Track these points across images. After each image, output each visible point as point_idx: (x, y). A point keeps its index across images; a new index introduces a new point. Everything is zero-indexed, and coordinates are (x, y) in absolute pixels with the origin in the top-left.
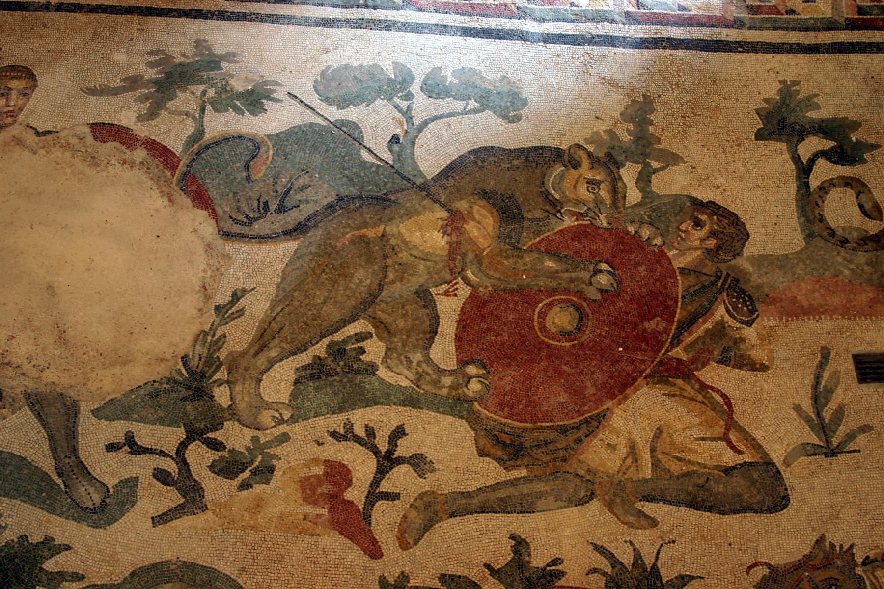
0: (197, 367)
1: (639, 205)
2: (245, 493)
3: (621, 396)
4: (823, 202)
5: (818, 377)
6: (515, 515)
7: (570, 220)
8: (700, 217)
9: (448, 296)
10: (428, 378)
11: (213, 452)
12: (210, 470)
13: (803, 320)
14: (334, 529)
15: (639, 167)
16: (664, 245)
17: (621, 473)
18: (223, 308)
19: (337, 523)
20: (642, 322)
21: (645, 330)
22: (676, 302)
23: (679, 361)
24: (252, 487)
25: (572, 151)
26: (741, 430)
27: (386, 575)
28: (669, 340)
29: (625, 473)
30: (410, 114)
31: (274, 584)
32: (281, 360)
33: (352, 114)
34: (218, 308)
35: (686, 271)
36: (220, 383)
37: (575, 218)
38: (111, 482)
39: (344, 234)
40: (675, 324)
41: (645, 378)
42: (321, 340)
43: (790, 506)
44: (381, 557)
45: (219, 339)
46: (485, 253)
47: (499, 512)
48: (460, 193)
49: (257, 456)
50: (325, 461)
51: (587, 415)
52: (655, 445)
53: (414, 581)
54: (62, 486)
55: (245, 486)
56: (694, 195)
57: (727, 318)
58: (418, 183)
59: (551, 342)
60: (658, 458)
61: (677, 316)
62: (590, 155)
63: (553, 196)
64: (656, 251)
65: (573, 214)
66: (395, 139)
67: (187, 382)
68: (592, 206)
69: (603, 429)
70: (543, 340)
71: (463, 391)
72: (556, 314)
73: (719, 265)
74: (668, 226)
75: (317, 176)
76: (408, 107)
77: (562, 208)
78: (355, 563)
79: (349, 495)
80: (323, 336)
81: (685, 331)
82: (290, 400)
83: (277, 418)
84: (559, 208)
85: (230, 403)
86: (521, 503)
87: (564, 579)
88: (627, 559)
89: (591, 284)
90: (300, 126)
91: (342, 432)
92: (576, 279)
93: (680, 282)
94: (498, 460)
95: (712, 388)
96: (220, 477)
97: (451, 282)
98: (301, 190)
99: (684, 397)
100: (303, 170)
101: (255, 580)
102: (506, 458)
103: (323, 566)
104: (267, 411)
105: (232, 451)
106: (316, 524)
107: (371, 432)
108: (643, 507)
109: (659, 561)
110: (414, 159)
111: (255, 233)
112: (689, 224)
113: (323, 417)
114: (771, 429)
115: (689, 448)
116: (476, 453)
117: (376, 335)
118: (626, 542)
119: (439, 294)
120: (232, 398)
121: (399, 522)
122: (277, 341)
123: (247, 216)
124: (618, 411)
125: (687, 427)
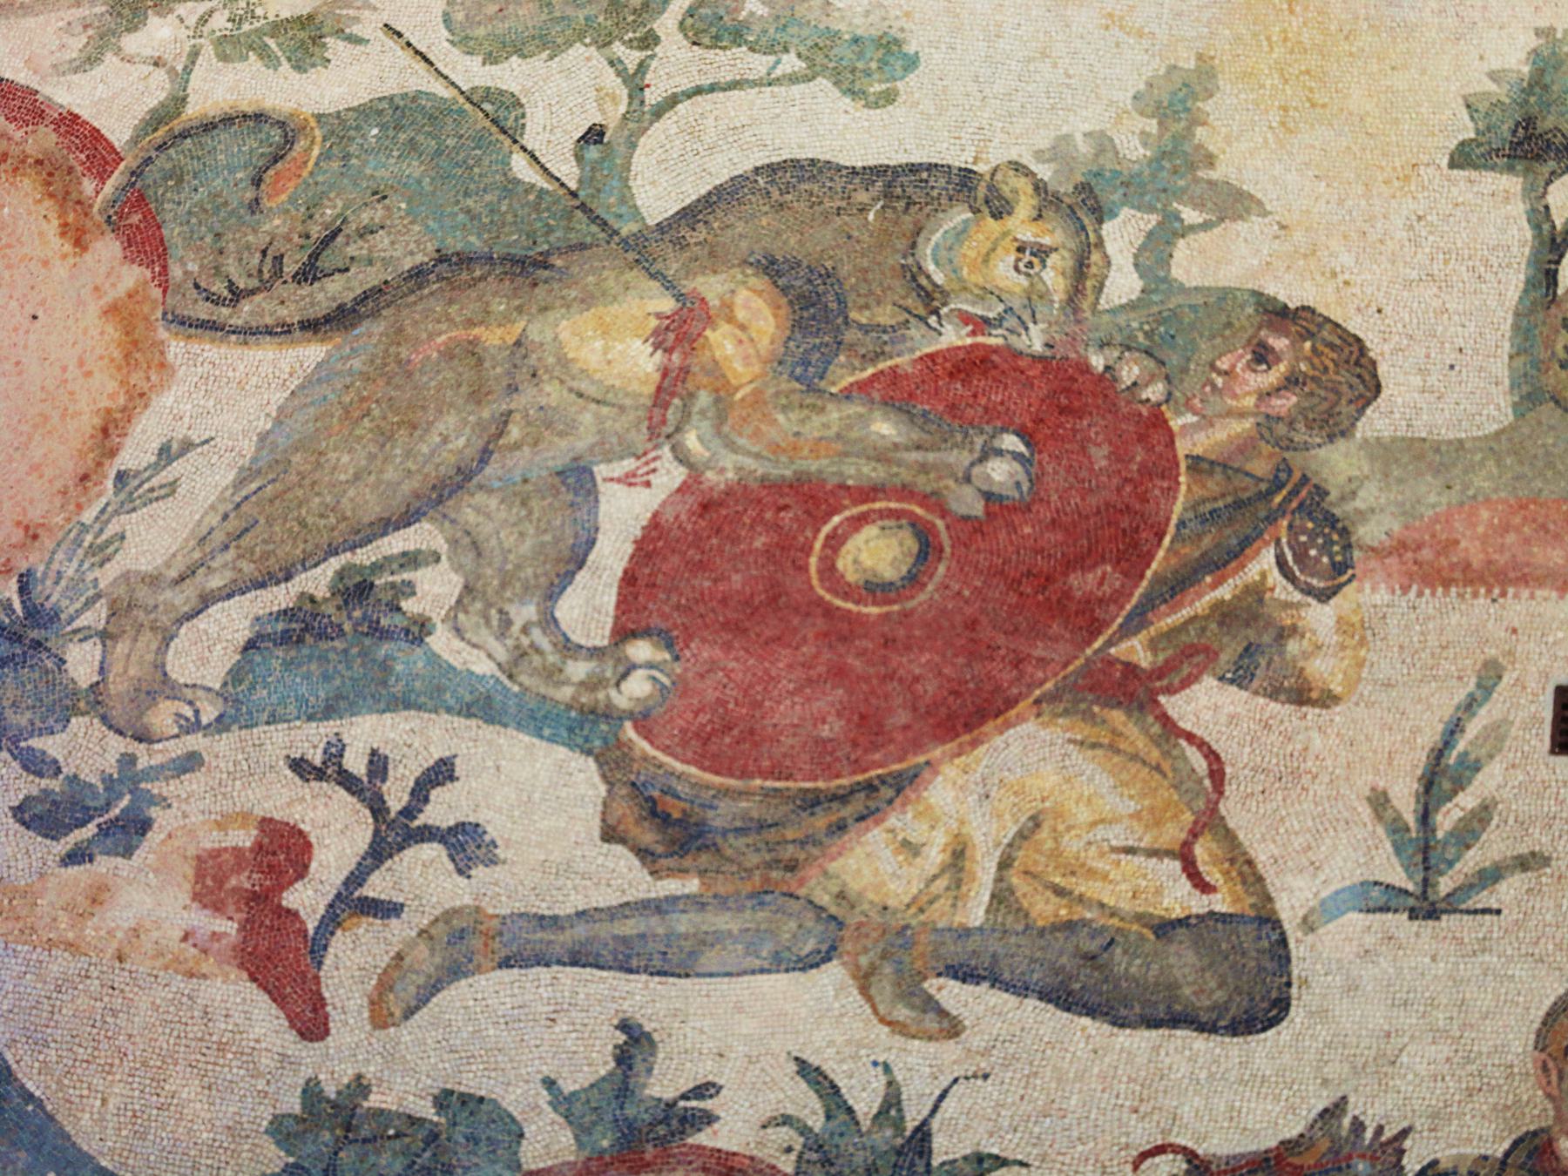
0: (48, 598)
1: (1131, 306)
2: (74, 870)
3: (966, 738)
5: (1454, 729)
6: (644, 977)
7: (957, 333)
8: (1271, 341)
9: (630, 484)
10: (537, 660)
11: (31, 777)
12: (15, 816)
13: (1461, 596)
14: (241, 966)
15: (1154, 219)
16: (1167, 401)
17: (913, 910)
18: (135, 477)
19: (250, 954)
20: (1066, 574)
21: (1067, 594)
22: (1160, 536)
23: (1131, 669)
24: (91, 861)
25: (999, 177)
26: (1230, 837)
27: (322, 1077)
28: (1120, 620)
29: (922, 910)
30: (642, 79)
31: (79, 1071)
32: (229, 596)
33: (510, 76)
34: (121, 477)
35: (1205, 466)
36: (84, 635)
37: (970, 328)
39: (431, 337)
41: (1037, 702)
42: (325, 560)
43: (1284, 1024)
44: (322, 1039)
45: (109, 542)
46: (739, 396)
47: (610, 968)
48: (715, 258)
49: (120, 796)
50: (264, 820)
51: (873, 773)
52: (1014, 854)
53: (379, 1097)
55: (76, 857)
56: (1271, 289)
57: (1275, 576)
58: (624, 232)
59: (839, 602)
61: (1154, 565)
62: (1039, 187)
63: (928, 277)
64: (1145, 412)
66: (595, 135)
67: (16, 628)
69: (904, 805)
70: (821, 598)
71: (608, 697)
72: (867, 542)
73: (1287, 455)
74: (1188, 360)
75: (403, 206)
76: (641, 65)
77: (944, 304)
78: (264, 1045)
80: (333, 551)
81: (1165, 601)
82: (225, 684)
83: (187, 719)
84: (936, 303)
85: (96, 678)
86: (665, 953)
87: (709, 1130)
88: (865, 1100)
89: (968, 479)
90: (391, 99)
91: (318, 762)
92: (935, 467)
94: (643, 853)
95: (1190, 737)
96: (31, 833)
97: (645, 454)
98: (361, 236)
99: (1118, 751)
100: (375, 193)
101: (41, 1058)
102: (660, 849)
103: (193, 1044)
104: (168, 703)
105: (74, 779)
106: (205, 952)
107: (378, 764)
108: (940, 989)
109: (938, 1116)
110: (627, 179)
111: (240, 322)
112: (1241, 356)
114: (1298, 842)
115: (1089, 870)
116: (597, 833)
117: (449, 558)
118: (875, 1064)
119: (612, 480)
120: (102, 668)
121: (383, 965)
122: (230, 555)
124: (950, 771)
125: (1102, 821)
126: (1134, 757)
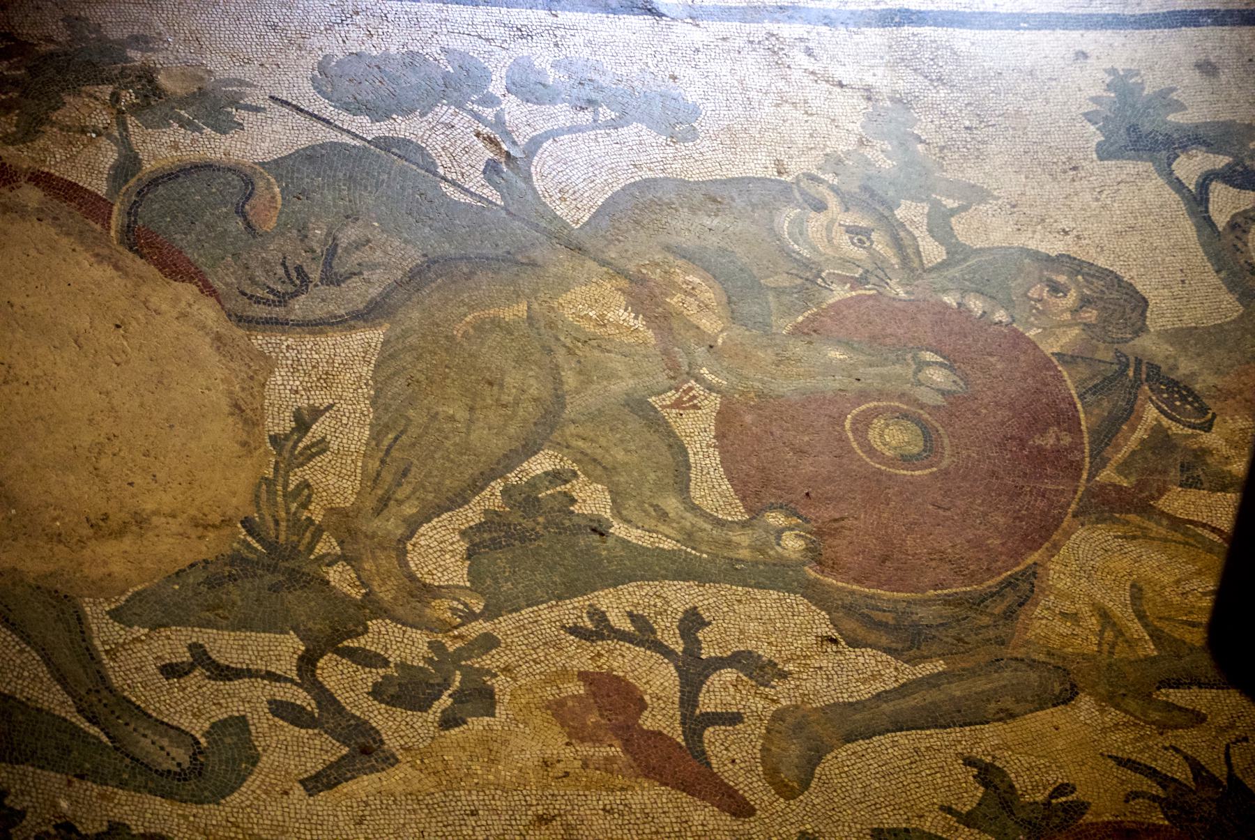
4: (1246, 245)
11: (367, 670)
33: (401, 127)
37: (848, 285)
38: (198, 728)
40: (1086, 435)
54: (105, 739)
57: (1165, 422)
60: (1155, 626)
61: (1083, 423)
62: (834, 189)
65: (843, 280)
68: (870, 267)
75: (376, 224)
79: (648, 722)
81: (1107, 445)
88: (1182, 773)
93: (1065, 374)
94: (888, 650)
105: (402, 666)
108: (1167, 696)
112: (1042, 290)
113: (545, 605)
118: (1166, 749)
123: (272, 291)
126: (1165, 540)
